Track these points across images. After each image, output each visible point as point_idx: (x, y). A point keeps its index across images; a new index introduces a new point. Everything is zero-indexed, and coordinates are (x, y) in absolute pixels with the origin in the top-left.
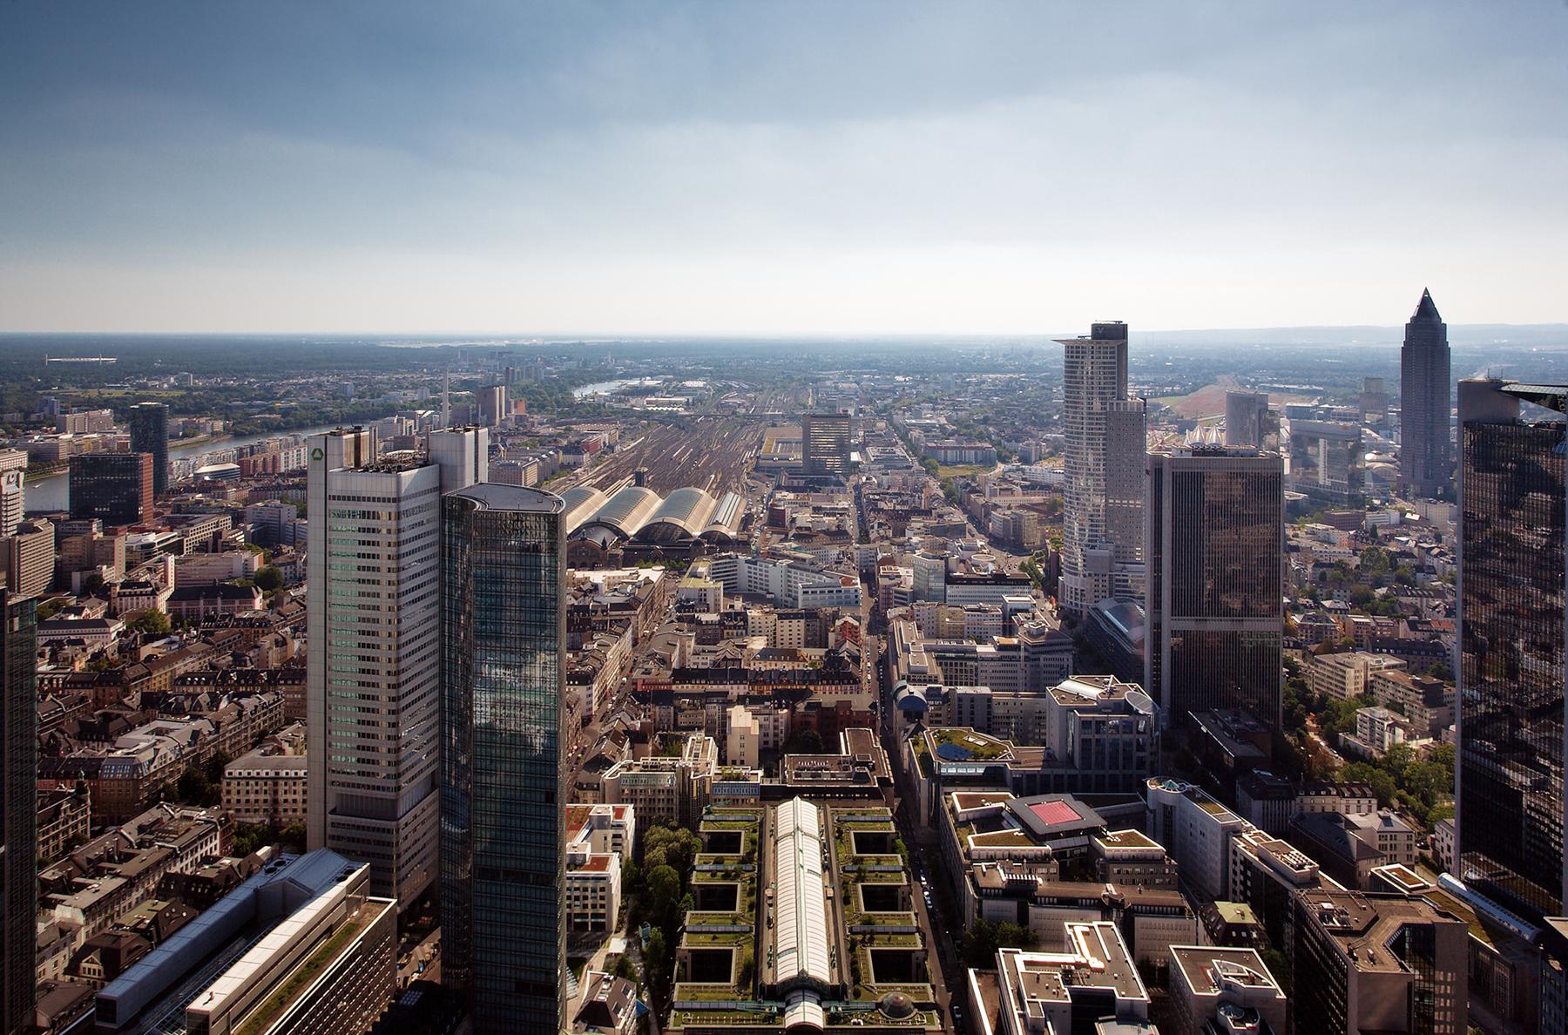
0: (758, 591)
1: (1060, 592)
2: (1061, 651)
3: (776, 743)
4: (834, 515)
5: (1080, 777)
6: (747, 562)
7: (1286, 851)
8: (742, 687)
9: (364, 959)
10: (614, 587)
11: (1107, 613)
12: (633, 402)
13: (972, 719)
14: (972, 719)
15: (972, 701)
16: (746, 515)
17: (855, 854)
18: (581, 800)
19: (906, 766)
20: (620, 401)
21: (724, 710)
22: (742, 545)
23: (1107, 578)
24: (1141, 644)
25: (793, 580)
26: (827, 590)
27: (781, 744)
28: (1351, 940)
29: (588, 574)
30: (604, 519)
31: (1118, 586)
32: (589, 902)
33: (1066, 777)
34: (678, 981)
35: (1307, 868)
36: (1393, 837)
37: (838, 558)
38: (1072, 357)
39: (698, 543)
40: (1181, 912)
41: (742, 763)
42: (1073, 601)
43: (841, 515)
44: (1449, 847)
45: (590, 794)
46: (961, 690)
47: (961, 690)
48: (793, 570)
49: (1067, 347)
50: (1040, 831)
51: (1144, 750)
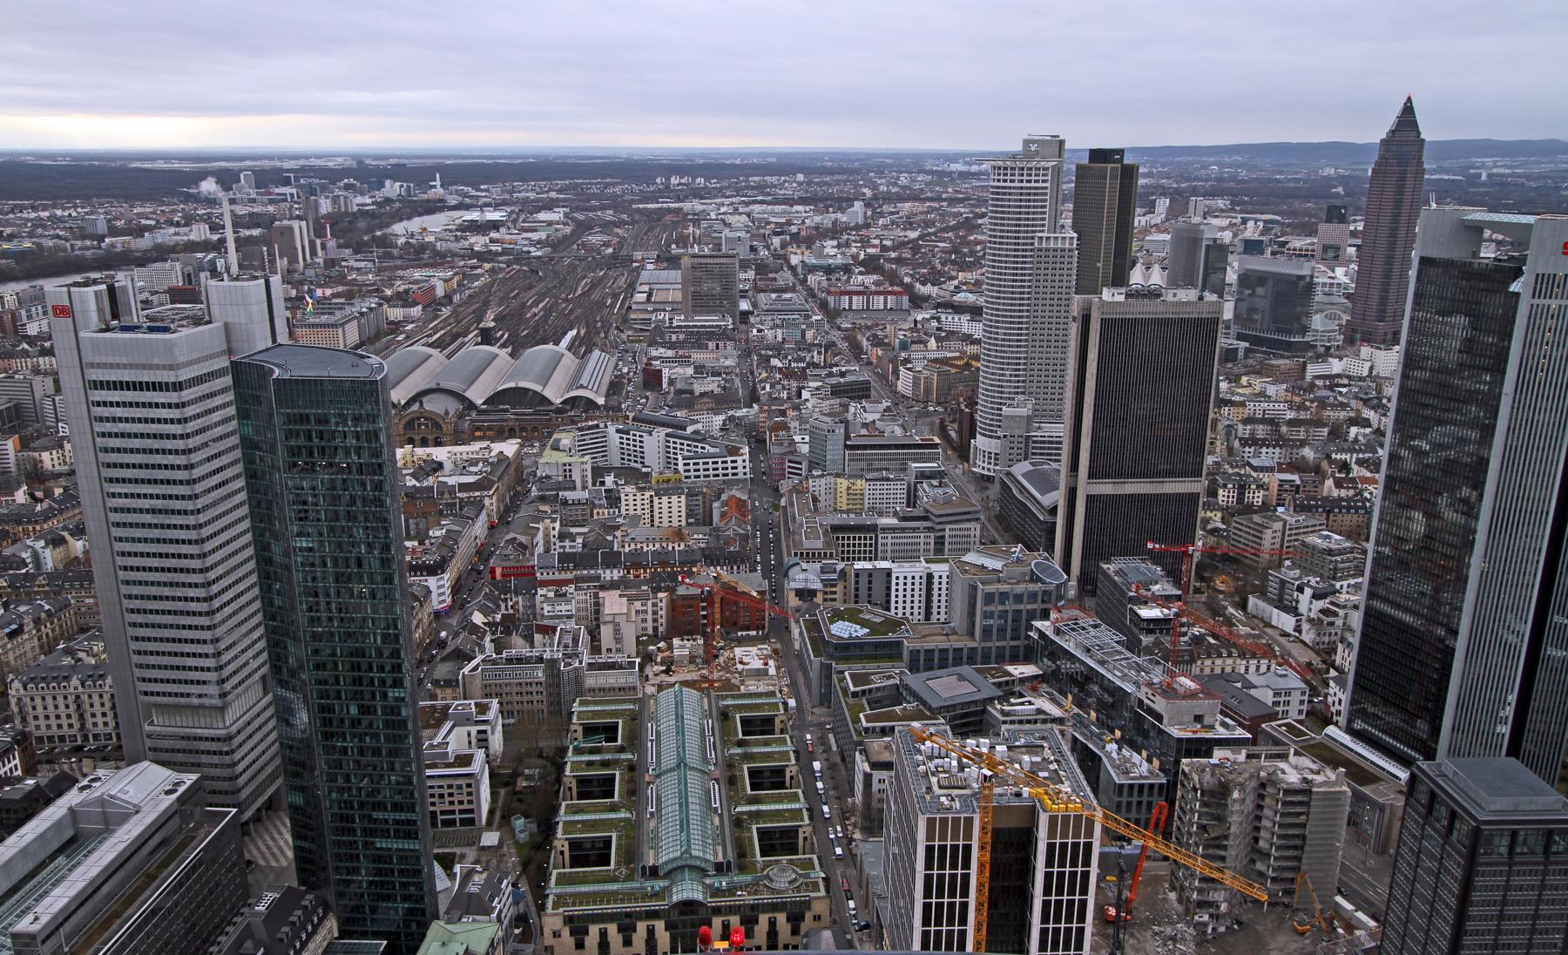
0: (633, 464)
2: (969, 520)
3: (655, 629)
4: (719, 374)
5: (980, 650)
6: (618, 431)
8: (615, 571)
9: (207, 869)
10: (462, 468)
12: (473, 240)
13: (870, 596)
14: (870, 596)
15: (870, 575)
16: (616, 377)
17: (740, 736)
18: (439, 697)
19: (797, 647)
20: (457, 239)
21: (596, 596)
22: (612, 411)
24: (1053, 511)
25: (671, 450)
26: (710, 461)
27: (660, 629)
29: (428, 450)
30: (445, 385)
32: (456, 799)
33: (965, 651)
34: (555, 868)
36: (1288, 694)
37: (724, 424)
39: (559, 411)
41: (618, 651)
42: (985, 465)
43: (727, 374)
44: (1340, 701)
45: (449, 691)
46: (859, 565)
47: (859, 565)
48: (672, 440)
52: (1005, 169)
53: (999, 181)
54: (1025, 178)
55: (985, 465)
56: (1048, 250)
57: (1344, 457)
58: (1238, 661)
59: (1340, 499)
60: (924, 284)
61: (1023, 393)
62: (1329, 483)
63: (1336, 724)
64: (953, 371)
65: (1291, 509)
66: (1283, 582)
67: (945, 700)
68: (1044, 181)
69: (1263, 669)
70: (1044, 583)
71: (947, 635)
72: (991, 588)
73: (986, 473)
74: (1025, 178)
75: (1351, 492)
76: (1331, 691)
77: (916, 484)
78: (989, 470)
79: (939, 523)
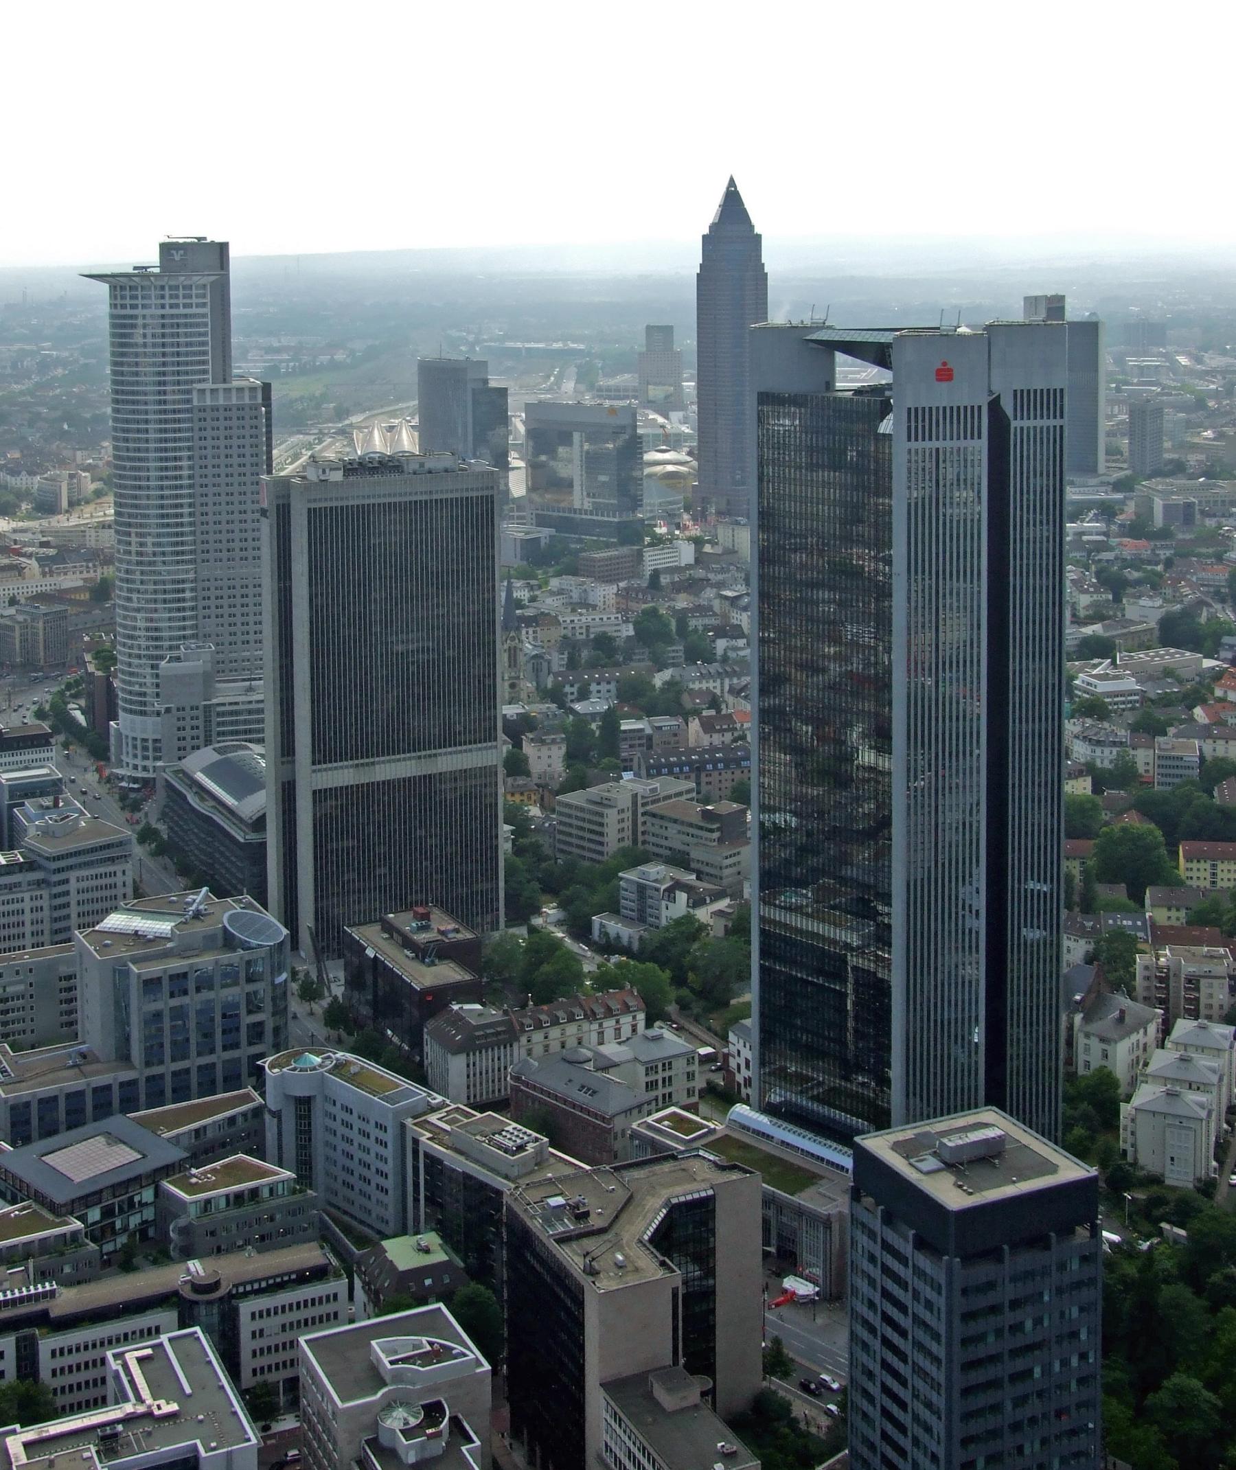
1: (113, 749)
7: (496, 1127)
11: (200, 777)
23: (200, 713)
24: (259, 824)
28: (589, 1244)
33: (116, 1089)
35: (530, 1148)
38: (123, 307)
40: (319, 1273)
42: (139, 762)
49: (113, 288)
50: (60, 1198)
51: (259, 1009)
55: (139, 762)
57: (711, 685)
58: (586, 1026)
59: (713, 749)
61: (195, 636)
62: (695, 725)
63: (747, 1101)
64: (71, 610)
65: (643, 772)
66: (641, 889)
67: (82, 1184)
69: (626, 1031)
70: (246, 947)
71: (75, 1066)
72: (154, 969)
75: (728, 737)
76: (733, 1049)
77: (11, 807)
78: (145, 769)
79: (59, 871)
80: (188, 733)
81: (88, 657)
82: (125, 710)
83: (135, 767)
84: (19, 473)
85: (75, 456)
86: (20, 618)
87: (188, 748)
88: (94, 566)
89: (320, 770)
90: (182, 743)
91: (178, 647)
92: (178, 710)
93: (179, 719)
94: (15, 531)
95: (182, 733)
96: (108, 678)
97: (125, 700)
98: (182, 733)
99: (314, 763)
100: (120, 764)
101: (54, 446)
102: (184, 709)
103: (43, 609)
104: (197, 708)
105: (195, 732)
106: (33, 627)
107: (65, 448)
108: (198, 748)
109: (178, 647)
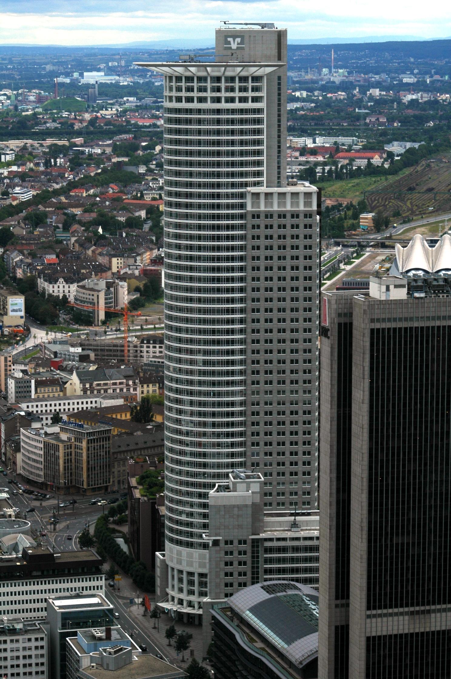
1: (158, 581)
23: (247, 547)
31: (270, 561)
42: (183, 596)
52: (189, 79)
53: (179, 99)
54: (223, 94)
56: (269, 215)
60: (52, 280)
61: (241, 465)
68: (255, 100)
73: (189, 610)
74: (223, 94)
77: (64, 636)
78: (190, 604)
80: (235, 568)
81: (133, 481)
82: (172, 540)
83: (181, 602)
84: (56, 281)
85: (110, 262)
86: (64, 437)
87: (236, 585)
88: (134, 383)
89: (374, 616)
90: (229, 579)
91: (227, 476)
92: (226, 543)
93: (226, 553)
94: (55, 342)
95: (229, 569)
96: (154, 504)
97: (171, 530)
98: (229, 569)
99: (369, 608)
100: (165, 598)
101: (90, 252)
102: (232, 543)
103: (88, 428)
104: (245, 542)
105: (242, 568)
106: (76, 447)
107: (101, 254)
108: (245, 585)
109: (227, 476)
